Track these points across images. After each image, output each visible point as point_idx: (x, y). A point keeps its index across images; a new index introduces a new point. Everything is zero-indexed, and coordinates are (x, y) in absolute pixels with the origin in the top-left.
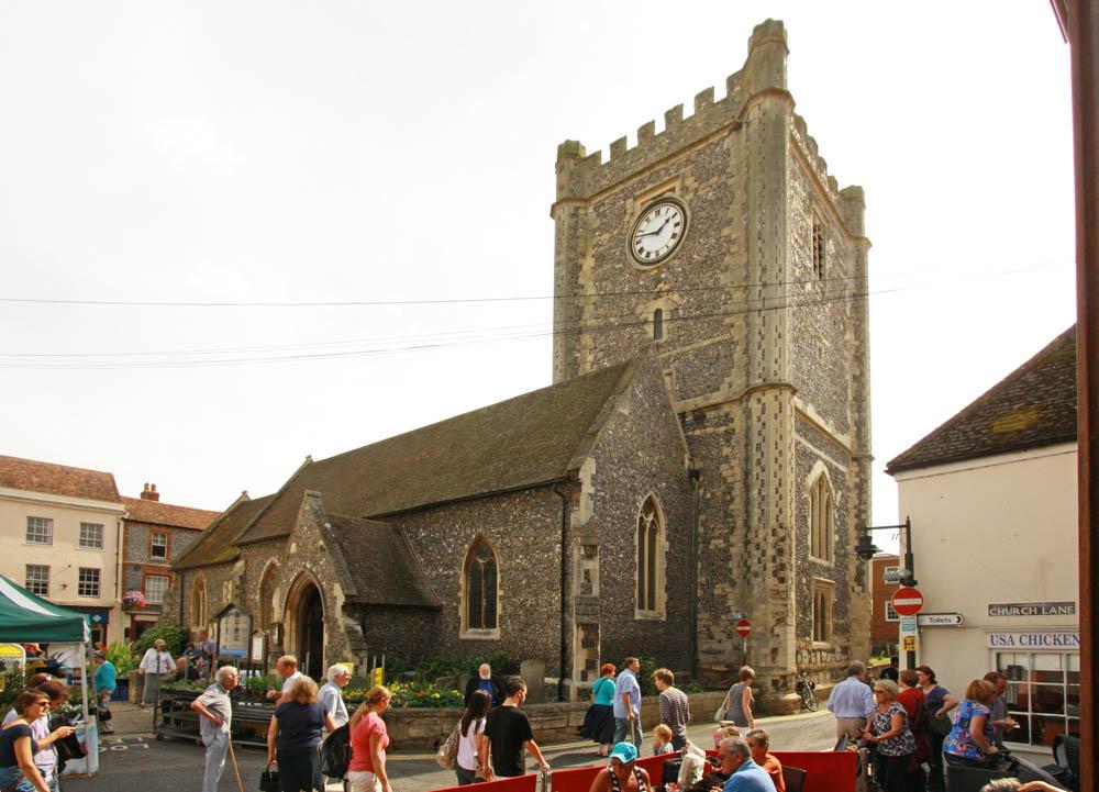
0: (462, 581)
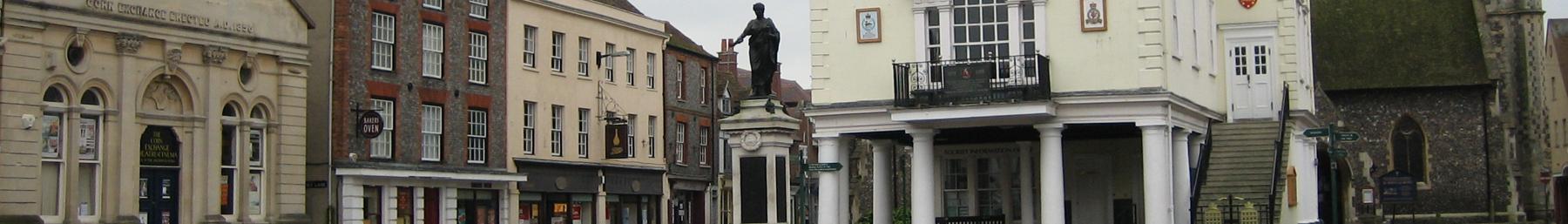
0: (1389, 147)
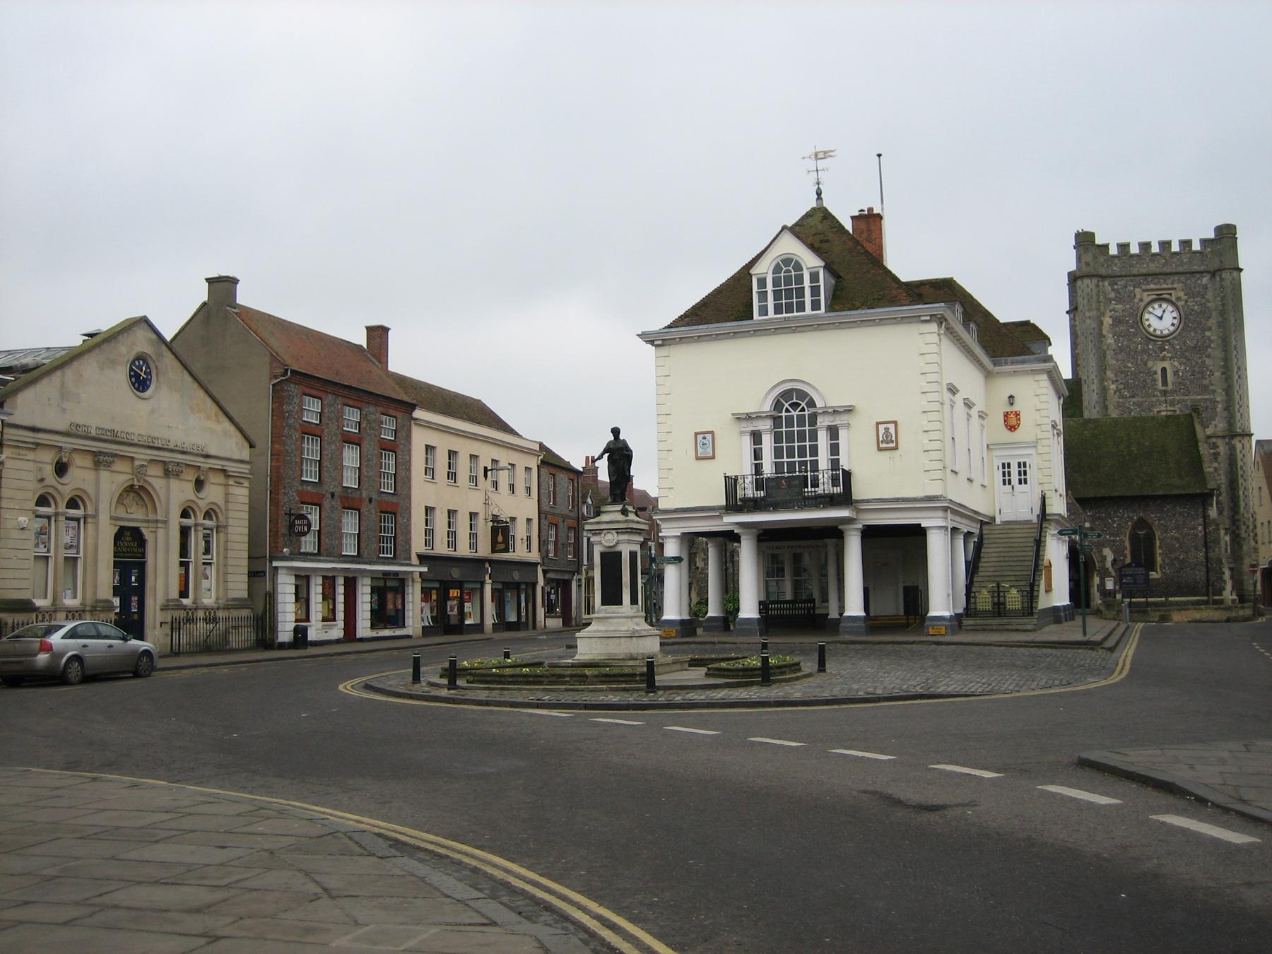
0: (1127, 544)
